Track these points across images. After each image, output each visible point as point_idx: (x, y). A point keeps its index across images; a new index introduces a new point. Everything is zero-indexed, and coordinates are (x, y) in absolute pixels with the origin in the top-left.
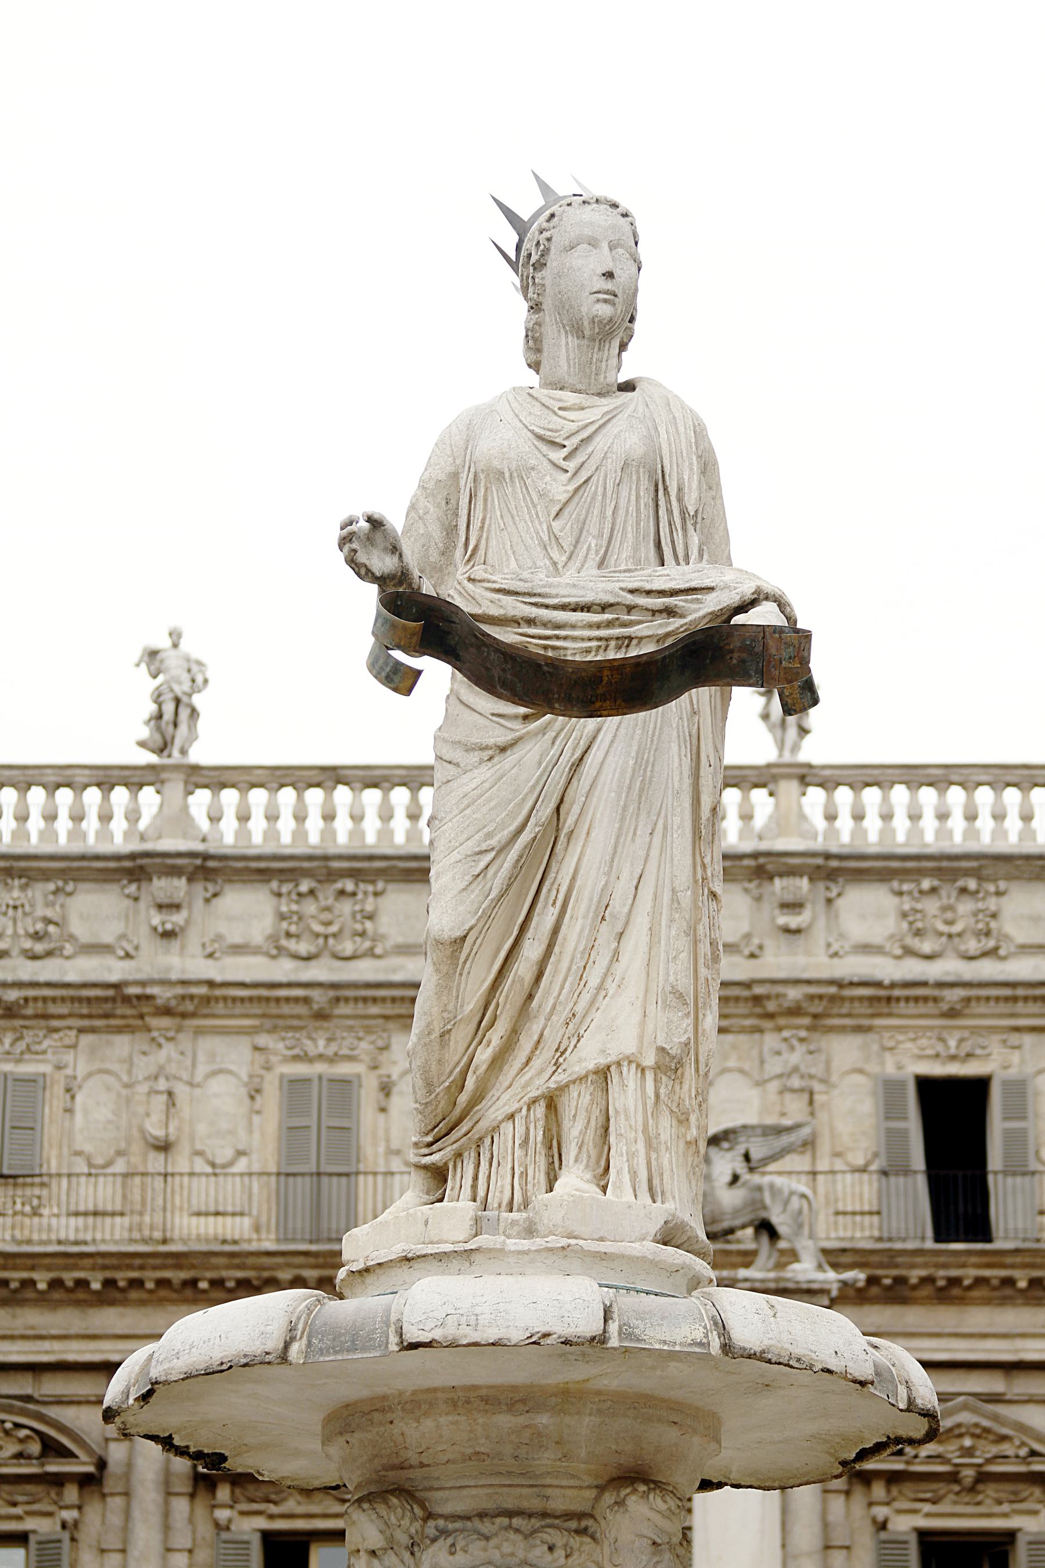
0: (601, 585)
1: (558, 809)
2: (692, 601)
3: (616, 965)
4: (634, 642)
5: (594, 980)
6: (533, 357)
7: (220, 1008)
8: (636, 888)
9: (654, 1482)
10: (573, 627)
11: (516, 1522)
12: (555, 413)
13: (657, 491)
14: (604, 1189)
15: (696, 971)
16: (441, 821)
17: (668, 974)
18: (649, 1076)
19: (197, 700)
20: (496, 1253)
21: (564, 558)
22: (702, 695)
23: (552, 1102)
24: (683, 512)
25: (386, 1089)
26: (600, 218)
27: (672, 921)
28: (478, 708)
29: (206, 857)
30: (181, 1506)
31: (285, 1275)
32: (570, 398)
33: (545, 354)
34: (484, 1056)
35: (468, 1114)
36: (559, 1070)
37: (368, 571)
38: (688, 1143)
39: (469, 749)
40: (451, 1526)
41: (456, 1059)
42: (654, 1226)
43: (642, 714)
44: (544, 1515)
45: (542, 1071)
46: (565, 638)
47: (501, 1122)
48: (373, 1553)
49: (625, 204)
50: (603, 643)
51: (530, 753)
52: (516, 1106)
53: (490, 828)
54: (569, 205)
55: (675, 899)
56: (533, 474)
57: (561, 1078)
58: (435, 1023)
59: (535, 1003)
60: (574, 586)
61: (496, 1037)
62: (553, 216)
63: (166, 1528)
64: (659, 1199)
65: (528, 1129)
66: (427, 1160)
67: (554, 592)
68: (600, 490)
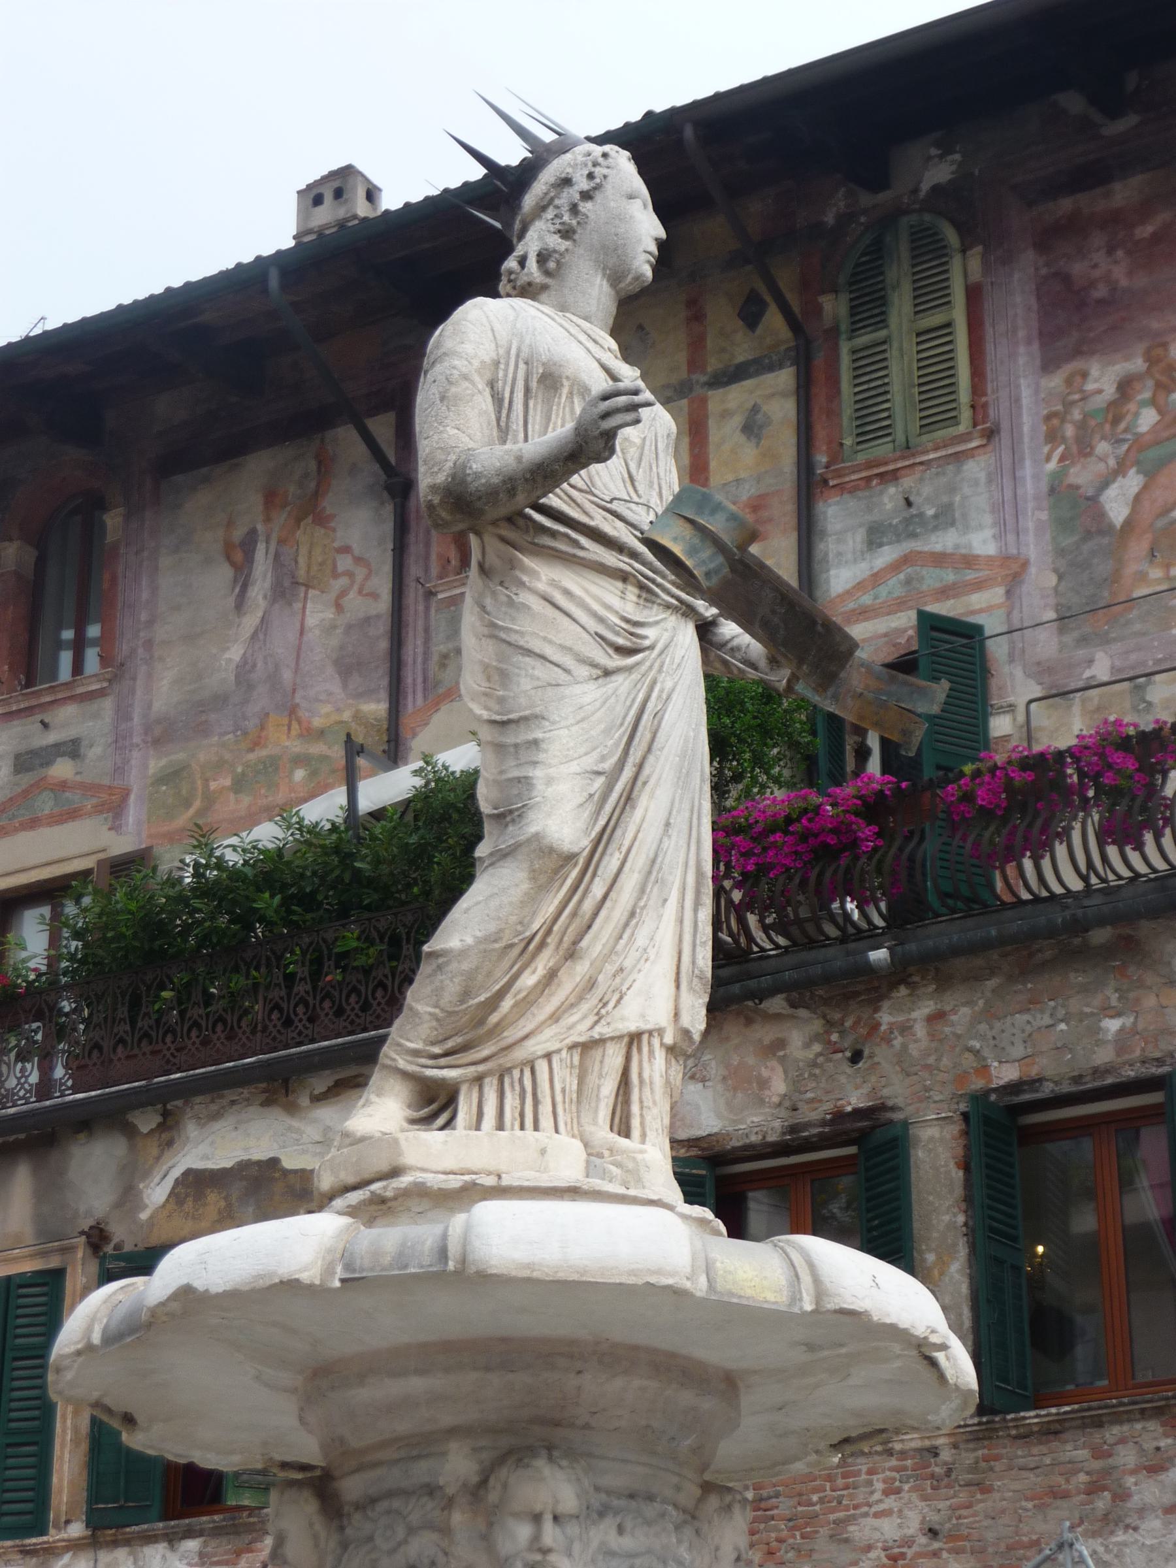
16: (553, 723)
36: (603, 1022)
45: (584, 1017)
57: (601, 1030)
58: (507, 931)
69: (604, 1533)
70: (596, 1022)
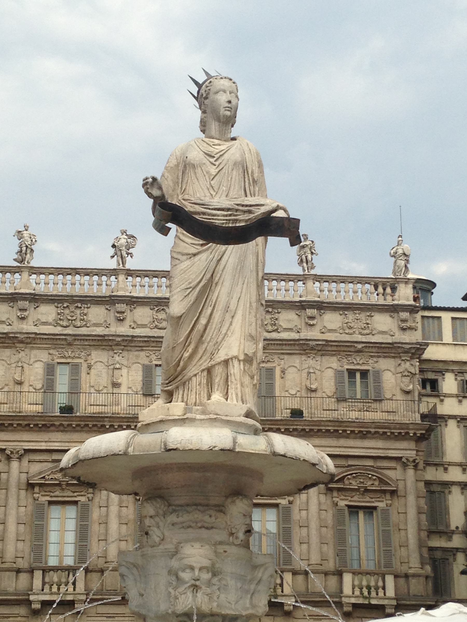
0: (228, 203)
1: (212, 275)
2: (257, 209)
3: (231, 326)
4: (238, 221)
5: (224, 331)
6: (203, 128)
7: (38, 341)
8: (238, 301)
9: (245, 495)
10: (218, 216)
11: (199, 507)
12: (211, 146)
13: (244, 172)
14: (227, 399)
15: (256, 329)
17: (249, 330)
18: (242, 363)
19: (33, 247)
20: (193, 420)
21: (215, 193)
22: (260, 240)
23: (209, 370)
24: (254, 180)
25: (90, 367)
26: (226, 83)
27: (250, 313)
28: (186, 242)
29: (35, 295)
30: (23, 493)
31: (57, 423)
32: (216, 142)
33: (207, 127)
34: (186, 355)
35: (180, 374)
37: (152, 195)
38: (254, 385)
39: (183, 254)
40: (177, 508)
41: (177, 356)
42: (243, 412)
43: (244, 244)
44: (207, 505)
45: (206, 360)
46: (216, 219)
47: (192, 377)
48: (151, 517)
49: (234, 80)
50: (228, 222)
51: (203, 256)
52: (197, 372)
53: (190, 281)
54: (216, 79)
55: (251, 305)
56: (204, 166)
57: (213, 363)
59: (204, 339)
60: (219, 202)
61: (190, 350)
62: (210, 82)
63: (18, 499)
64: (245, 403)
65: (201, 379)
66: (166, 388)
67: (212, 204)
68: (227, 172)
69: (173, 518)
70: (210, 361)
